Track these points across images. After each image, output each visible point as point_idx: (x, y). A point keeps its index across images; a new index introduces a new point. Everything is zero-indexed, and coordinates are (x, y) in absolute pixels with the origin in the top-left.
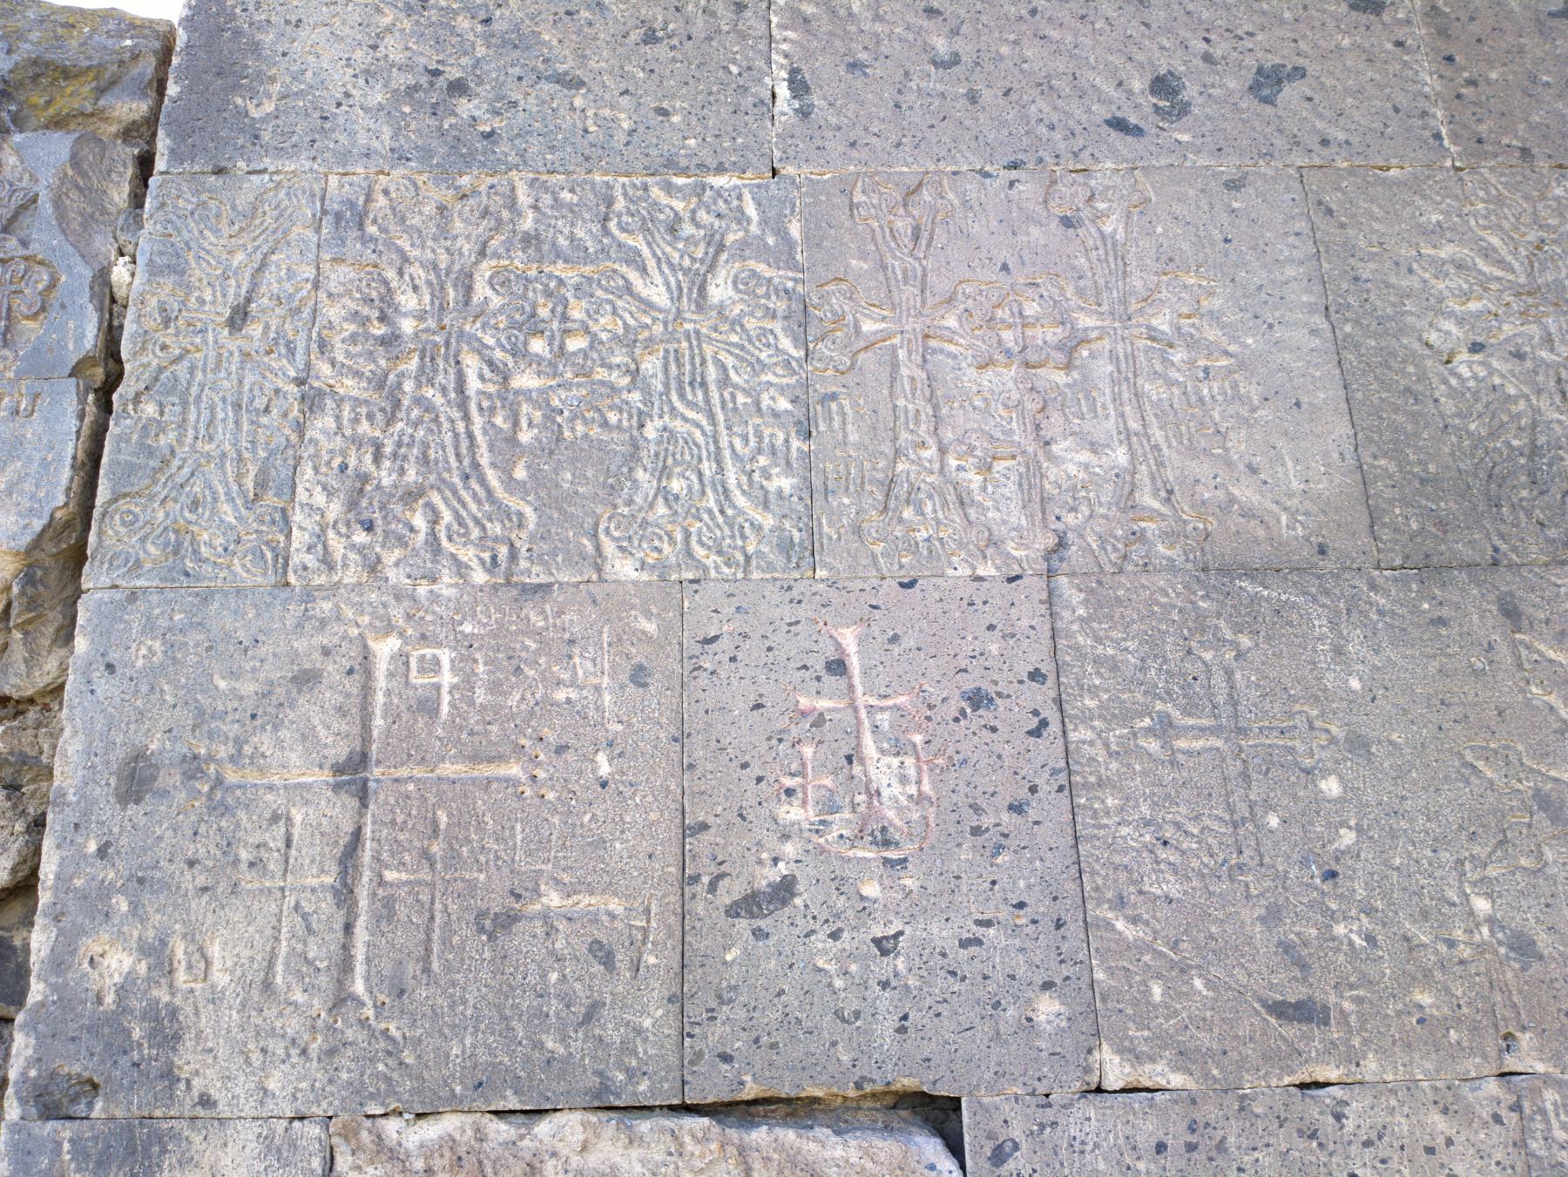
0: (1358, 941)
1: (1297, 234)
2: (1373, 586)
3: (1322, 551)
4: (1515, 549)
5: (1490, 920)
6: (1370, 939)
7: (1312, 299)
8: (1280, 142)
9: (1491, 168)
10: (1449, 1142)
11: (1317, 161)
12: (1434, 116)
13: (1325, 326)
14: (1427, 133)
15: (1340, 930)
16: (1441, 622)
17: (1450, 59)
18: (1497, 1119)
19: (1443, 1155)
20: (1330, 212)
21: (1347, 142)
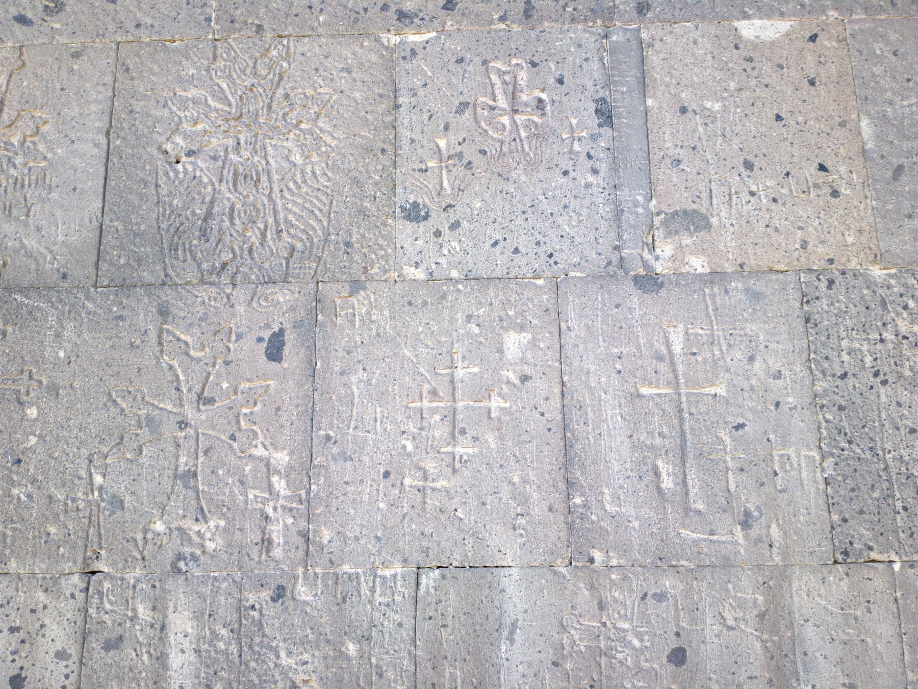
0: (23, 498)
1: (104, 85)
2: (88, 298)
3: (64, 276)
4: (178, 275)
5: (101, 488)
6: (30, 496)
7: (101, 125)
8: (111, 27)
9: (235, 39)
10: (45, 607)
11: (130, 38)
12: (211, 6)
13: (105, 141)
14: (203, 18)
15: (15, 491)
16: (121, 318)
18: (73, 596)
19: (40, 615)
20: (127, 70)
21: (152, 26)
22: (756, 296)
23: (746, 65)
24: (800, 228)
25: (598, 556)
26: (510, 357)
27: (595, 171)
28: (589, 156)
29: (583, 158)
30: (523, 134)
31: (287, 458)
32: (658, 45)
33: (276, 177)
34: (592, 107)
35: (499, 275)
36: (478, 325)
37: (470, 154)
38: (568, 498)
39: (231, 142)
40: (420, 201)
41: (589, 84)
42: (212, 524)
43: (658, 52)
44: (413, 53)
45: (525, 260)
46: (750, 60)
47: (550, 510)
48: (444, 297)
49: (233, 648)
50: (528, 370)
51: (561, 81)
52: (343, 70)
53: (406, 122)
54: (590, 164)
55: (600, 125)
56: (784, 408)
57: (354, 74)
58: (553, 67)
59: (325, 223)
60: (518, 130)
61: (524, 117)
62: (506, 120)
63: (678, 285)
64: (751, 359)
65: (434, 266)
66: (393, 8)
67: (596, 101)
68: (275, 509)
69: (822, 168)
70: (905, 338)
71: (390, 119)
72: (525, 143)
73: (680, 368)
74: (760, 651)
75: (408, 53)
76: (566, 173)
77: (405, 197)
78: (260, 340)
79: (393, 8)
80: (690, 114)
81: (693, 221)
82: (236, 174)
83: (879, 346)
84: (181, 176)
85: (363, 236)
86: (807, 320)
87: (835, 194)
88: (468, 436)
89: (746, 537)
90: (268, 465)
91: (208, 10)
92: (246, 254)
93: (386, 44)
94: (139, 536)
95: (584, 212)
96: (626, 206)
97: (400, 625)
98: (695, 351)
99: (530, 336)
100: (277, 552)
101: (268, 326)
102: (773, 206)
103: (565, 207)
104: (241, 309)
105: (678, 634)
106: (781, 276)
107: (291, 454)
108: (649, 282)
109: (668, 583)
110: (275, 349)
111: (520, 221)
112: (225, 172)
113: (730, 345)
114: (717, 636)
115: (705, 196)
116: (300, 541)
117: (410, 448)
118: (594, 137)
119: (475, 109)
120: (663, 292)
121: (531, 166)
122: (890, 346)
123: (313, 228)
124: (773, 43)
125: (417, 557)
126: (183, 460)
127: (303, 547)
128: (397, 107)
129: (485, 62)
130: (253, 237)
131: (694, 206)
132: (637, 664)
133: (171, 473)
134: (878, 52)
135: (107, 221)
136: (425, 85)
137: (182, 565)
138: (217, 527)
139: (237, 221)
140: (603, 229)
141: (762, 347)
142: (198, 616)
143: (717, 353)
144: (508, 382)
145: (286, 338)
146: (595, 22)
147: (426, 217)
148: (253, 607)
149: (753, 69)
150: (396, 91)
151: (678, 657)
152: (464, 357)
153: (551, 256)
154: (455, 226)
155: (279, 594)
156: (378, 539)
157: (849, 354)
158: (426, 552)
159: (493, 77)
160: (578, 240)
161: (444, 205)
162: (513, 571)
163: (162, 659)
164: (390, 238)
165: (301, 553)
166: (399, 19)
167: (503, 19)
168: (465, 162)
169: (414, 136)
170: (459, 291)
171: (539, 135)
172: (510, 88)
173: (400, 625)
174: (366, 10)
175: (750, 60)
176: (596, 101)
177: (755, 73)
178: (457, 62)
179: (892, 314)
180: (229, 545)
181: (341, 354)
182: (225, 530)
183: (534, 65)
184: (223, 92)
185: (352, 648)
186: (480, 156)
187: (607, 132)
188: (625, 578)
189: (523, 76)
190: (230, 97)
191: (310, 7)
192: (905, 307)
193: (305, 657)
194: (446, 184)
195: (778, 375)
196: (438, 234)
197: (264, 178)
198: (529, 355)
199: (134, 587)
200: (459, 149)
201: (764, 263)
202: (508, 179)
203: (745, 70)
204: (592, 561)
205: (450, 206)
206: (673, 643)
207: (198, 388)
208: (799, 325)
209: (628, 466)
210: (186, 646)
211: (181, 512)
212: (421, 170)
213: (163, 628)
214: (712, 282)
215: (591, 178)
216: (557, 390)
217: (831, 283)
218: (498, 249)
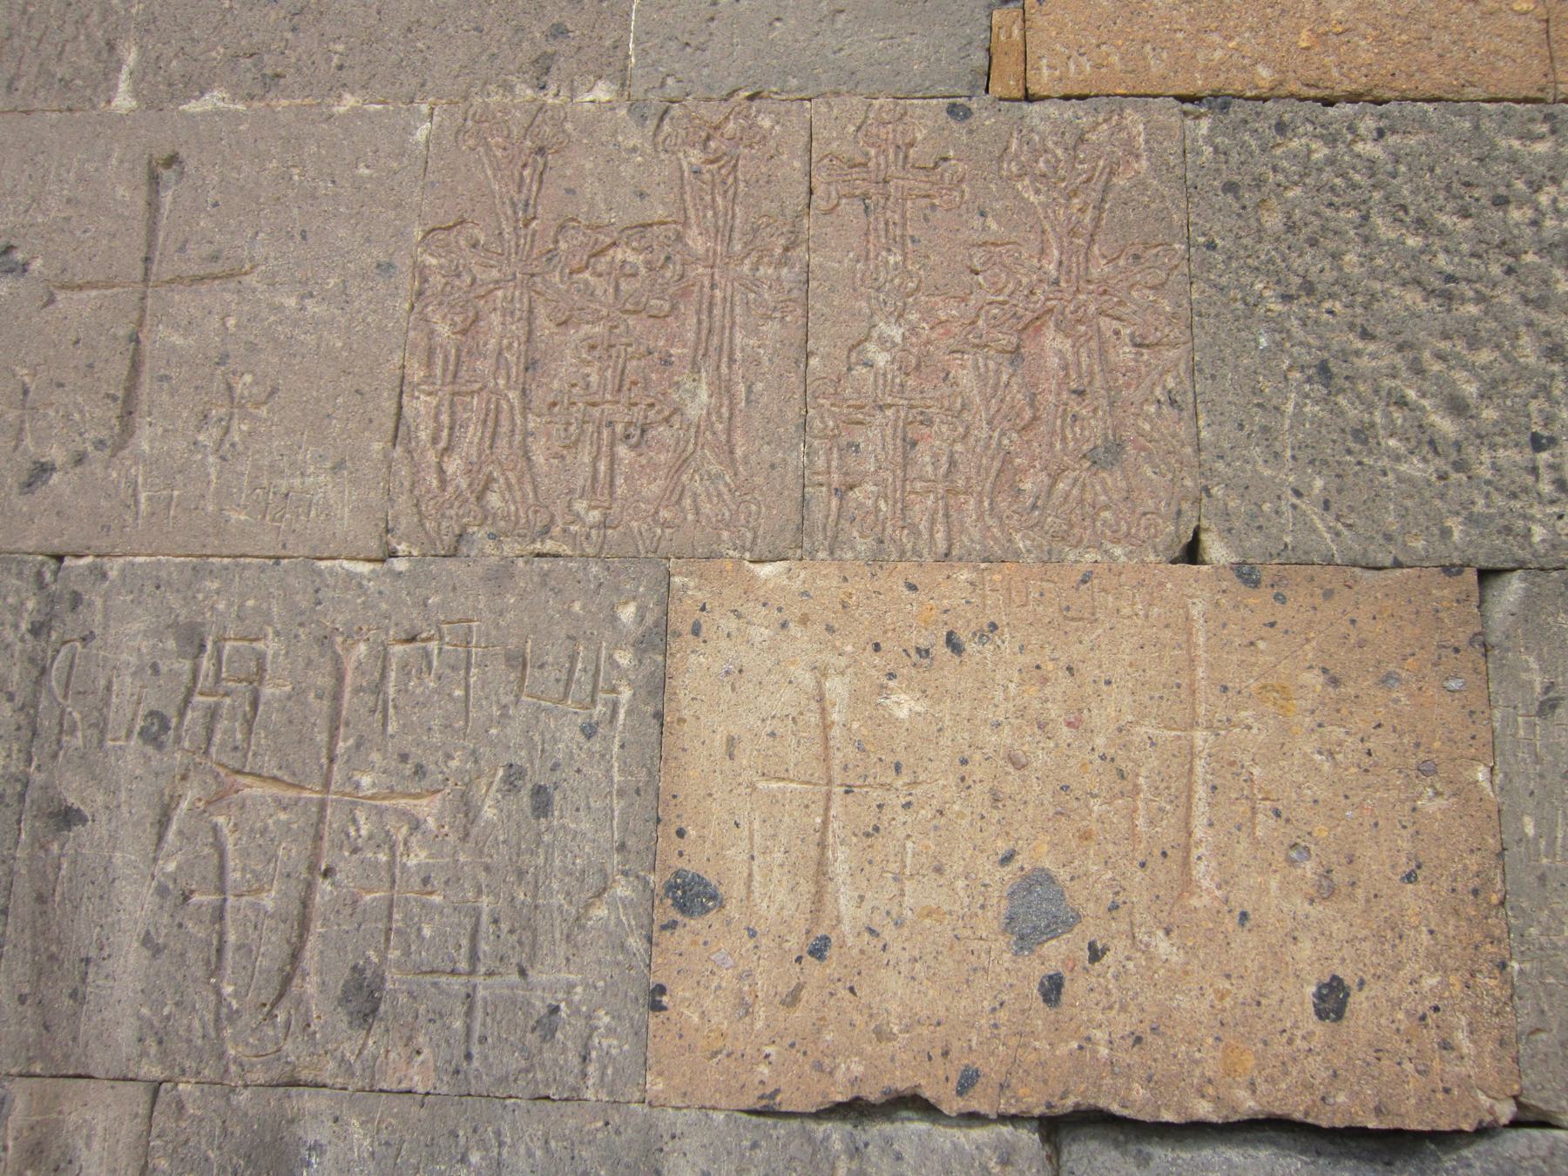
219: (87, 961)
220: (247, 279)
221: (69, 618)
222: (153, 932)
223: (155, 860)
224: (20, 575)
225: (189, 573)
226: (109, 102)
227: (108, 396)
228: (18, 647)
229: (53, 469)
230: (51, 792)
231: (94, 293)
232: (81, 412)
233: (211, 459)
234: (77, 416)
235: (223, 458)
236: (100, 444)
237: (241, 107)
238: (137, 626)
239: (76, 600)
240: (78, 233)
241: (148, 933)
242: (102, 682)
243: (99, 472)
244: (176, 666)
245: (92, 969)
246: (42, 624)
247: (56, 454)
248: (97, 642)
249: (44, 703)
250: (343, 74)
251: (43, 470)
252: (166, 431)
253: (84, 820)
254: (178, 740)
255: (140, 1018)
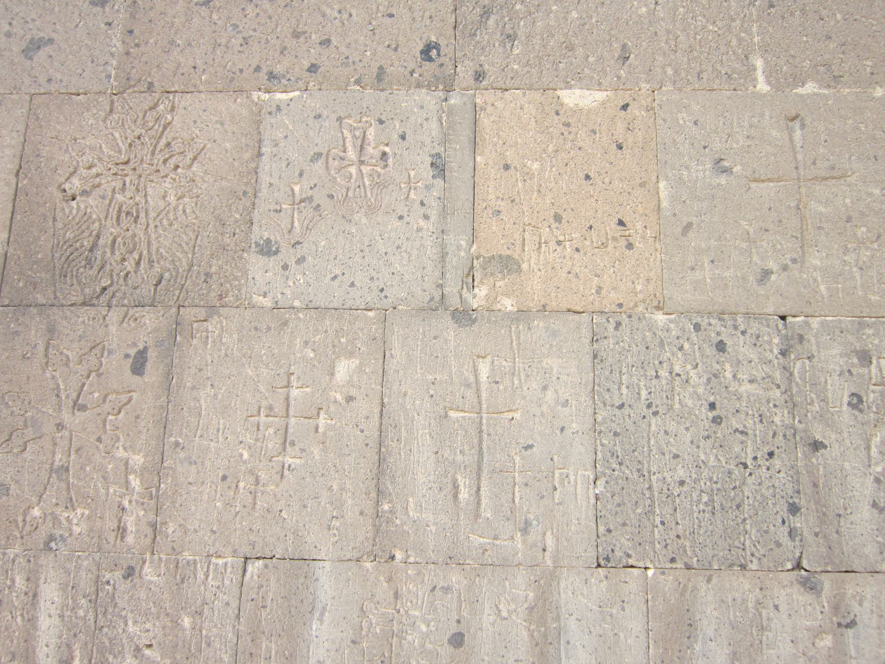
1: (18, 131)
7: (12, 167)
8: (27, 81)
11: (42, 91)
13: (14, 181)
14: (104, 75)
16: (16, 333)
17: (131, 32)
20: (37, 119)
21: (61, 81)
22: (554, 334)
23: (564, 129)
24: (597, 276)
25: (399, 555)
26: (339, 380)
27: (426, 217)
28: (422, 204)
29: (417, 204)
30: (367, 183)
31: (142, 460)
32: (489, 109)
33: (152, 215)
34: (429, 160)
35: (336, 305)
36: (313, 350)
37: (319, 197)
38: (377, 503)
39: (118, 184)
40: (272, 238)
41: (428, 141)
42: (79, 511)
43: (489, 115)
44: (279, 108)
45: (359, 293)
46: (568, 125)
47: (361, 513)
48: (285, 323)
49: (91, 616)
50: (353, 392)
51: (403, 137)
52: (217, 122)
53: (267, 168)
54: (422, 211)
55: (434, 177)
56: (568, 432)
57: (226, 126)
58: (397, 125)
59: (190, 256)
60: (363, 178)
61: (369, 168)
62: (353, 170)
63: (489, 321)
64: (545, 388)
65: (279, 296)
66: (265, 70)
67: (432, 156)
68: (130, 502)
69: (621, 223)
70: (678, 375)
71: (253, 165)
72: (368, 190)
73: (484, 395)
74: (526, 638)
75: (274, 109)
76: (401, 218)
77: (259, 233)
78: (127, 356)
79: (265, 70)
80: (512, 171)
81: (508, 265)
82: (120, 211)
83: (654, 382)
84: (75, 211)
85: (221, 268)
86: (595, 357)
87: (630, 246)
88: (297, 448)
89: (524, 542)
90: (127, 463)
91: (109, 68)
92: (121, 281)
93: (256, 100)
94: (20, 519)
95: (415, 252)
96: (450, 249)
97: (228, 604)
98: (498, 380)
99: (358, 362)
100: (130, 539)
101: (134, 344)
102: (576, 255)
103: (398, 247)
104: (113, 329)
105: (459, 621)
106: (577, 316)
107: (145, 456)
108: (464, 316)
109: (455, 578)
110: (139, 366)
111: (358, 259)
112: (111, 210)
113: (527, 376)
114: (493, 624)
115: (519, 243)
116: (149, 531)
117: (246, 456)
118: (428, 187)
119: (327, 159)
120: (475, 327)
121: (371, 210)
122: (664, 382)
123: (180, 259)
124: (589, 111)
125: (246, 550)
126: (58, 456)
127: (151, 535)
128: (260, 155)
129: (340, 119)
130: (130, 265)
131: (508, 252)
132: (423, 646)
133: (48, 467)
134: (681, 122)
135: (11, 250)
136: (286, 137)
137: (53, 545)
138: (83, 515)
139: (117, 253)
140: (429, 268)
141: (554, 379)
142: (63, 587)
143: (516, 382)
144: (335, 402)
145: (149, 354)
146: (437, 88)
147: (276, 252)
148: (108, 583)
149: (570, 133)
150: (260, 141)
151: (457, 640)
152: (299, 378)
153: (382, 290)
154: (301, 261)
155: (130, 573)
156: (214, 532)
157: (628, 387)
158: (253, 545)
159: (345, 132)
160: (406, 277)
161: (292, 242)
162: (327, 564)
163: (32, 621)
164: (245, 272)
165: (149, 540)
166: (269, 79)
167: (358, 82)
168: (314, 204)
169: (272, 181)
170: (299, 318)
171: (380, 185)
172: (359, 142)
173: (228, 604)
174: (241, 71)
175: (568, 125)
176: (432, 156)
177: (571, 137)
178: (315, 117)
179: (668, 354)
180: (91, 530)
181: (193, 370)
182: (89, 518)
183: (381, 122)
184: (115, 139)
185: (187, 622)
186: (328, 200)
187: (439, 182)
188: (419, 573)
189: (371, 133)
190: (121, 144)
191: (195, 68)
192: (681, 348)
193: (148, 626)
194: (296, 224)
195: (566, 403)
196: (285, 267)
197: (142, 215)
198: (355, 379)
199: (14, 561)
200: (310, 193)
201: (564, 306)
202: (350, 221)
203: (562, 134)
204: (393, 558)
205: (298, 243)
206: (454, 629)
207: (75, 395)
208: (587, 360)
209: (432, 478)
210: (53, 612)
211: (54, 501)
212: (276, 211)
213: (35, 595)
214: (518, 320)
215: (422, 223)
216: (377, 410)
217: (618, 324)
218: (337, 282)
219: (839, 515)
220: (848, 179)
221: (799, 347)
222: (877, 501)
223: (870, 466)
224: (768, 326)
225: (856, 326)
226: (755, 87)
227: (793, 236)
228: (776, 361)
229: (772, 273)
230: (809, 433)
231: (771, 184)
232: (781, 244)
233: (855, 269)
234: (779, 247)
235: (861, 269)
236: (794, 261)
237: (826, 92)
238: (835, 352)
239: (801, 338)
240: (757, 153)
241: (874, 501)
242: (823, 380)
243: (796, 273)
244: (860, 371)
245: (842, 519)
246: (786, 350)
247: (772, 265)
248: (816, 359)
249: (795, 390)
250: (874, 77)
251: (766, 274)
252: (827, 255)
253: (825, 447)
254: (869, 408)
255: (878, 542)
